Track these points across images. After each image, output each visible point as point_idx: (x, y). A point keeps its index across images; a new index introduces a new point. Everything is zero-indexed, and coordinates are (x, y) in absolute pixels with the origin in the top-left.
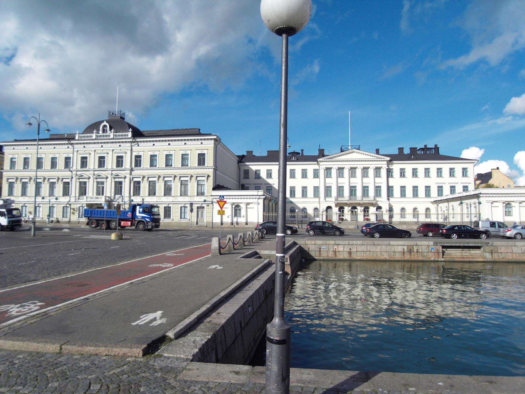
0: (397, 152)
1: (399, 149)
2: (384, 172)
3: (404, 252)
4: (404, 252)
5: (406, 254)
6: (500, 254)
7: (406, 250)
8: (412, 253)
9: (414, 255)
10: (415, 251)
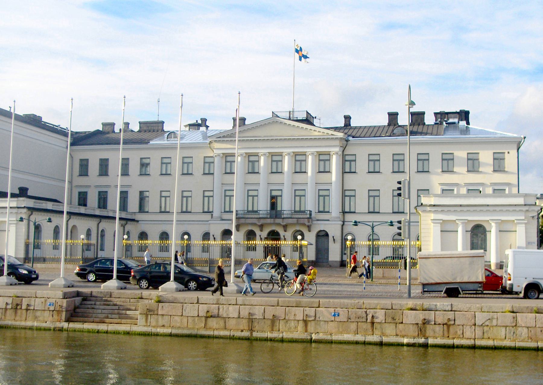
0: (384, 121)
1: (390, 114)
2: (335, 163)
3: (6, 309)
4: (6, 309)
5: (9, 312)
6: (160, 317)
7: (9, 307)
8: (19, 312)
9: (21, 313)
10: (24, 307)
